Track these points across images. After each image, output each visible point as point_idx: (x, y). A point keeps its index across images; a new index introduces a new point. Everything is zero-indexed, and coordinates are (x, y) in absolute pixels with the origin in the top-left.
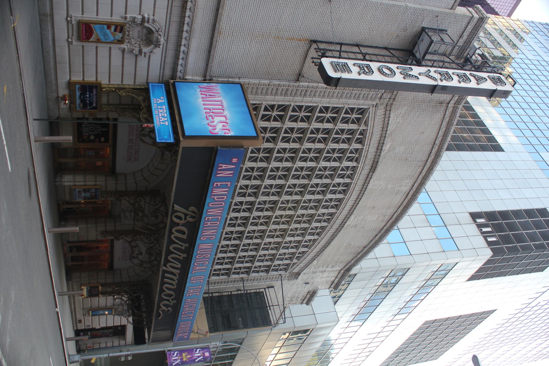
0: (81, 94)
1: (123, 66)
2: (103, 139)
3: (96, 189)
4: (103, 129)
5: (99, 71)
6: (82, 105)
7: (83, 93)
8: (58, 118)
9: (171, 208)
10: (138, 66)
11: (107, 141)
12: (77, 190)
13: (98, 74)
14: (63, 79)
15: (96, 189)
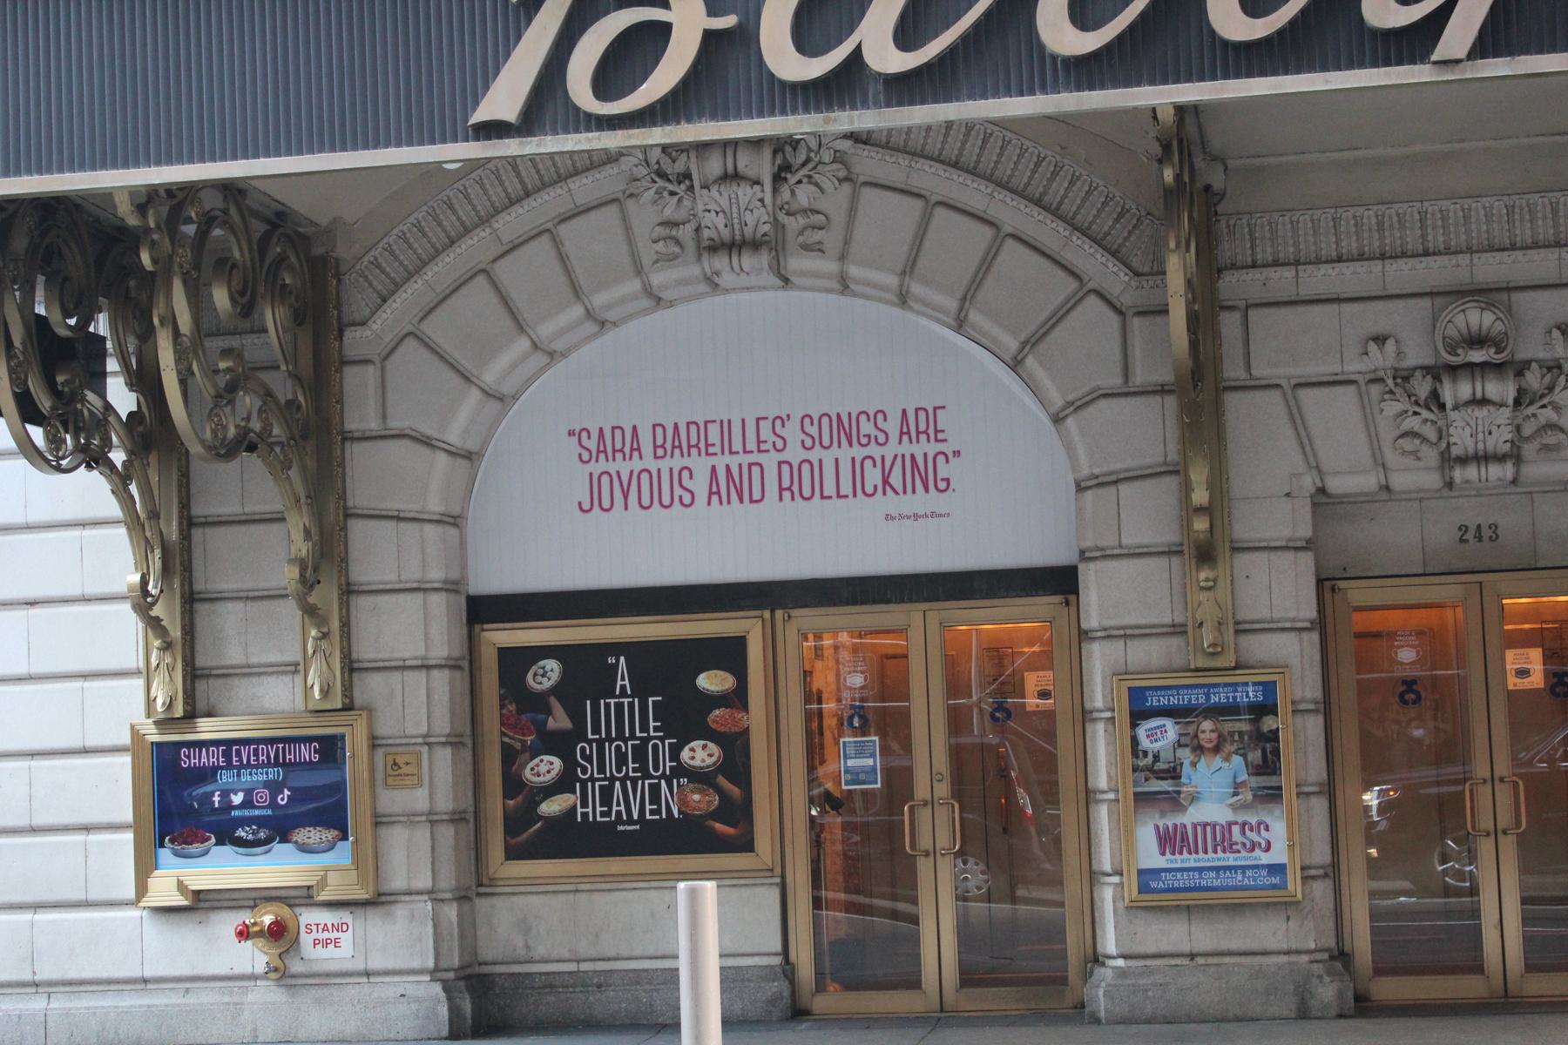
0: (226, 836)
1: (32, 603)
2: (711, 681)
3: (1139, 714)
4: (623, 681)
5: (76, 743)
6: (311, 835)
7: (226, 831)
8: (435, 973)
9: (511, 147)
10: (19, 519)
11: (730, 653)
12: (1150, 856)
13: (91, 742)
14: (134, 942)
15: (1139, 714)
